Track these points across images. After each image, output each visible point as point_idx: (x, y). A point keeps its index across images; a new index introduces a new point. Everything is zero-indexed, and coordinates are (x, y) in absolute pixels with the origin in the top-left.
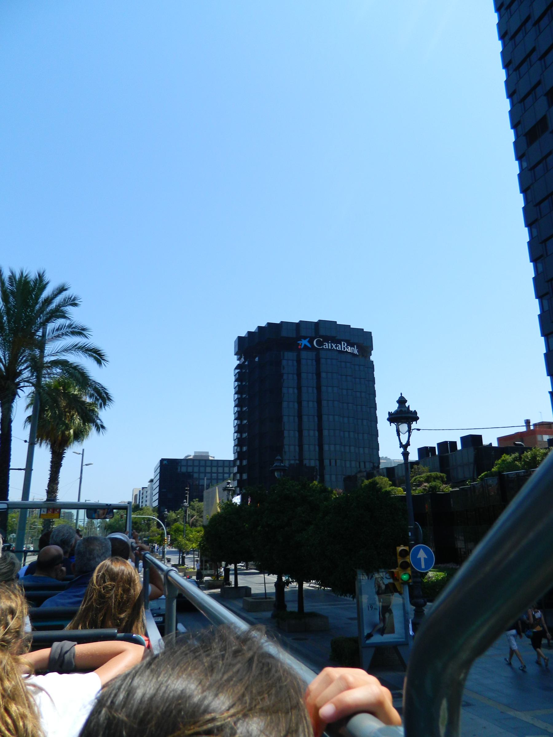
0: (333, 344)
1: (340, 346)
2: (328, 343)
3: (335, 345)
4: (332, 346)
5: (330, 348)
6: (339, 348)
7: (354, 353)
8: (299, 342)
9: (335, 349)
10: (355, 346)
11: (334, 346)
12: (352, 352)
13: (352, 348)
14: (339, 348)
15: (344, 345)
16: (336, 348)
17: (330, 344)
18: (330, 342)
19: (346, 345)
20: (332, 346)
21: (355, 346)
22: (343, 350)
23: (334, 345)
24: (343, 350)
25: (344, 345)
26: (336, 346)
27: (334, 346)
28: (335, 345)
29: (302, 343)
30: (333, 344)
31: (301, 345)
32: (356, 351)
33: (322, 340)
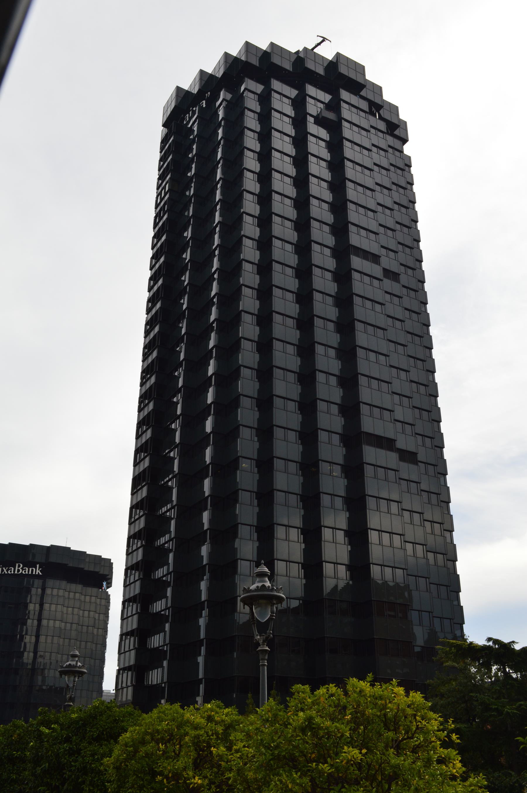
0: (4, 568)
1: (13, 569)
6: (11, 572)
7: (34, 573)
9: (6, 573)
10: (38, 566)
11: (5, 570)
12: (30, 573)
15: (19, 566)
16: (7, 572)
19: (21, 566)
21: (38, 566)
23: (5, 569)
24: (16, 572)
25: (19, 566)
26: (7, 571)
27: (5, 570)
30: (4, 568)
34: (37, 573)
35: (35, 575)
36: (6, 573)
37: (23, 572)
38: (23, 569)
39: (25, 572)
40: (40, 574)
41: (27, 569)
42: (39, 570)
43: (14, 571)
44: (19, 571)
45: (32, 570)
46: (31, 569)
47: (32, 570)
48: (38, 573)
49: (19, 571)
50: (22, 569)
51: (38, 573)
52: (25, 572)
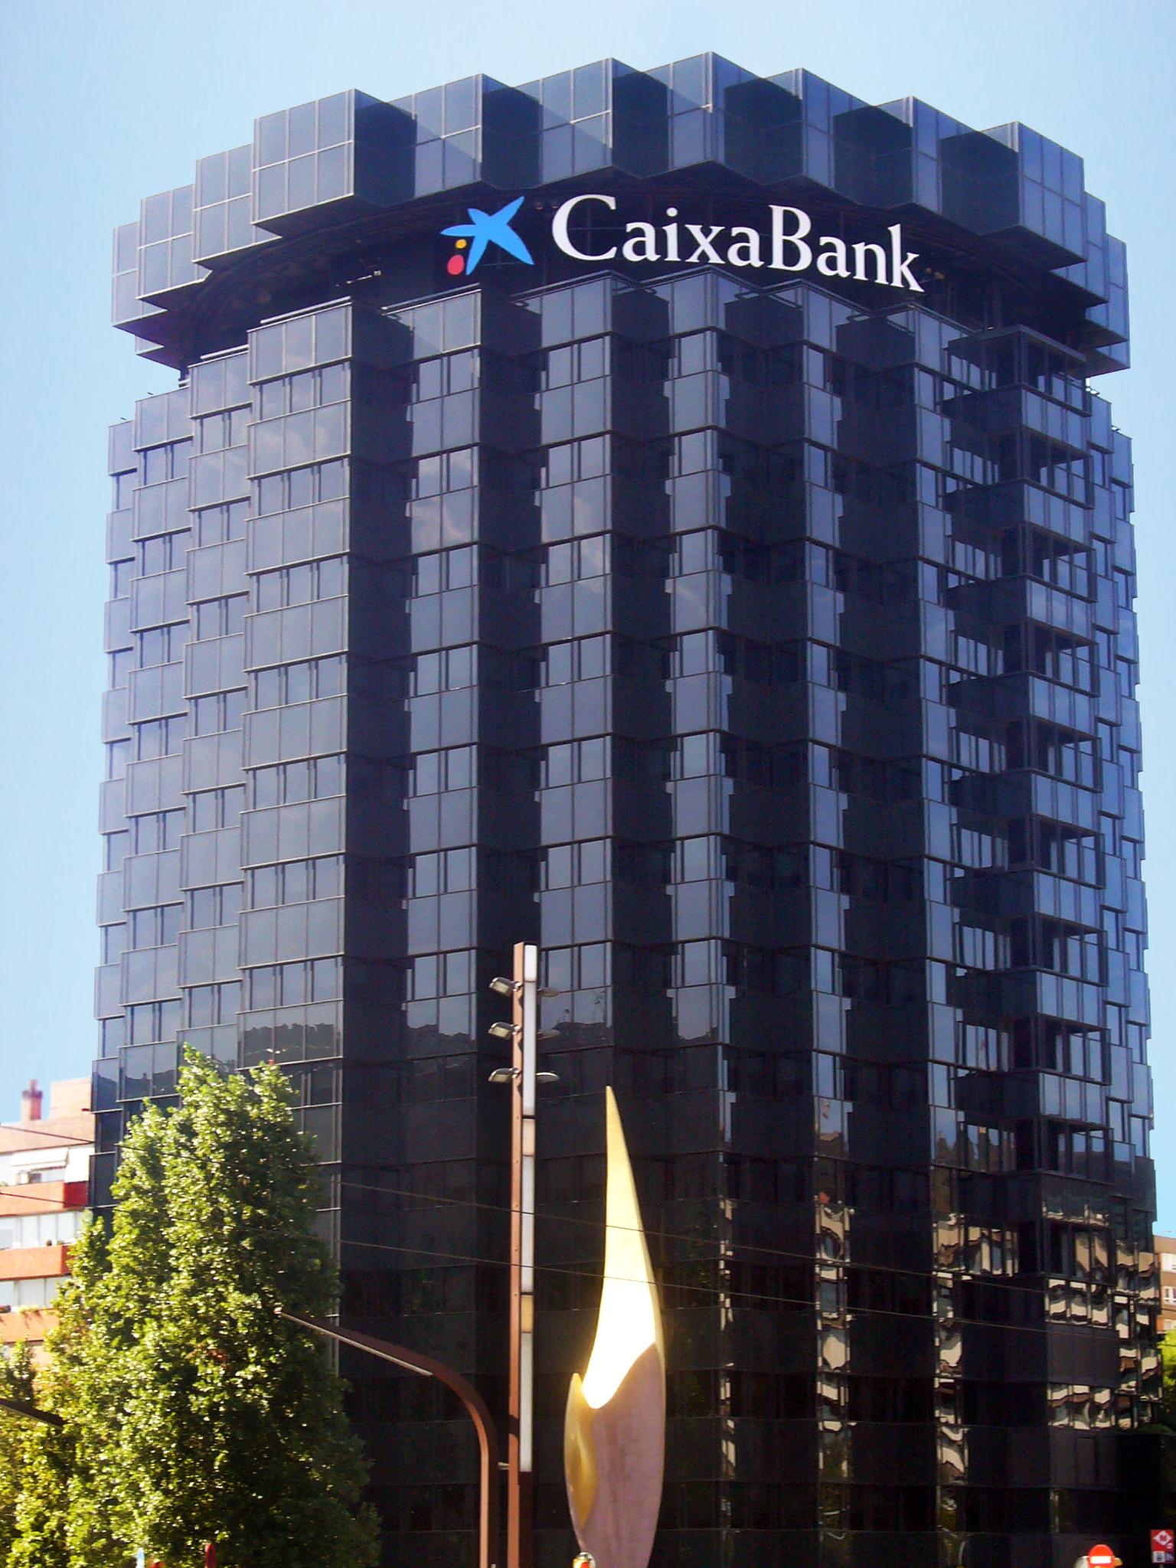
0: (695, 230)
1: (754, 236)
2: (660, 222)
3: (716, 230)
4: (687, 244)
5: (673, 256)
6: (744, 254)
7: (881, 279)
8: (449, 232)
9: (714, 258)
10: (895, 231)
11: (705, 244)
12: (860, 275)
13: (860, 249)
14: (744, 254)
15: (791, 225)
16: (723, 254)
17: (671, 230)
18: (672, 212)
20: (687, 244)
21: (895, 231)
22: (778, 263)
23: (706, 232)
24: (778, 263)
25: (791, 225)
26: (721, 245)
27: (705, 244)
28: (716, 230)
29: (470, 240)
30: (695, 230)
31: (465, 253)
32: (900, 269)
33: (611, 202)
34: (897, 282)
35: (888, 289)
36: (714, 258)
37: (823, 268)
38: (817, 251)
39: (832, 263)
40: (915, 286)
41: (840, 246)
42: (904, 258)
43: (766, 252)
44: (791, 254)
45: (870, 257)
46: (860, 249)
47: (870, 257)
48: (904, 280)
49: (791, 254)
50: (811, 240)
51: (904, 280)
52: (832, 263)
